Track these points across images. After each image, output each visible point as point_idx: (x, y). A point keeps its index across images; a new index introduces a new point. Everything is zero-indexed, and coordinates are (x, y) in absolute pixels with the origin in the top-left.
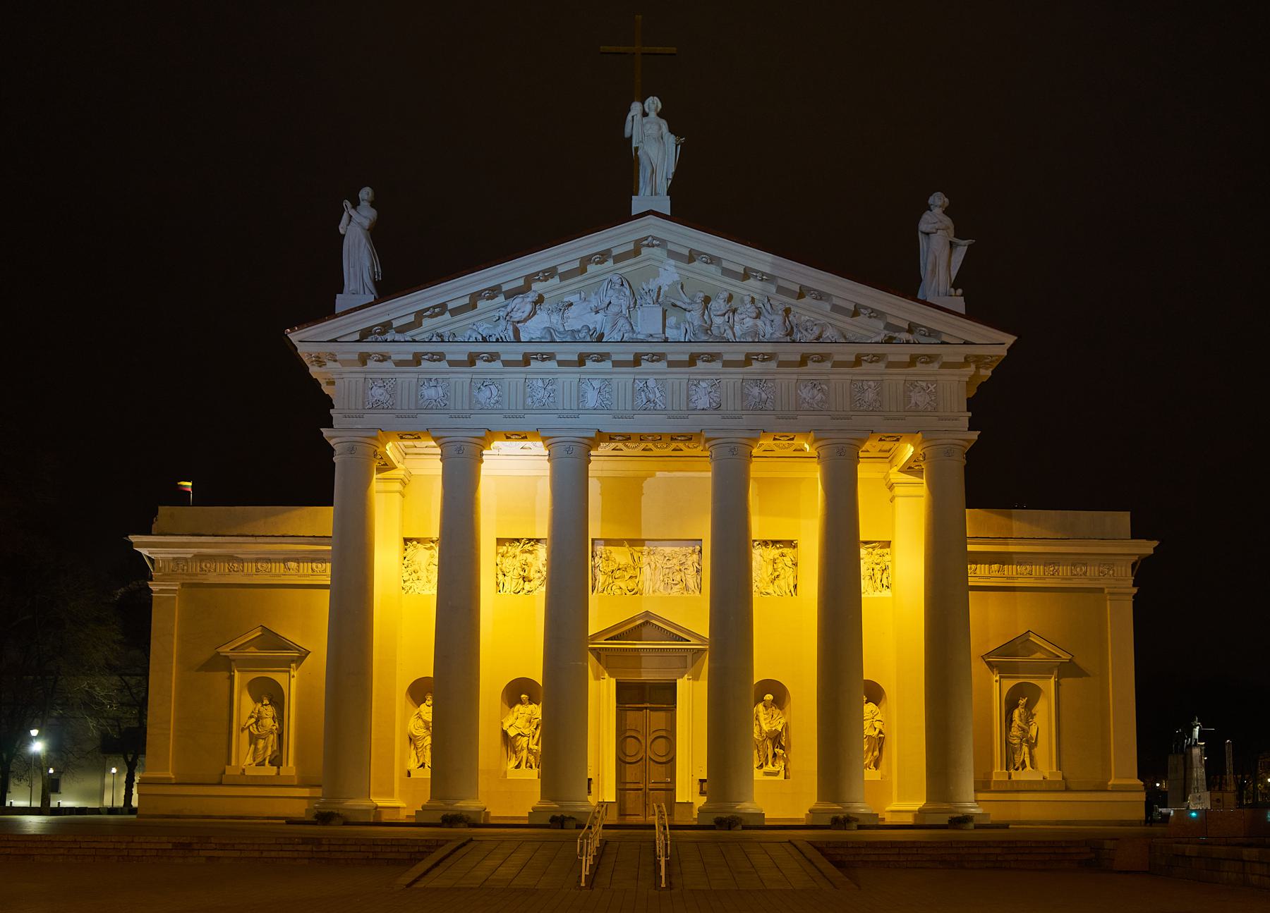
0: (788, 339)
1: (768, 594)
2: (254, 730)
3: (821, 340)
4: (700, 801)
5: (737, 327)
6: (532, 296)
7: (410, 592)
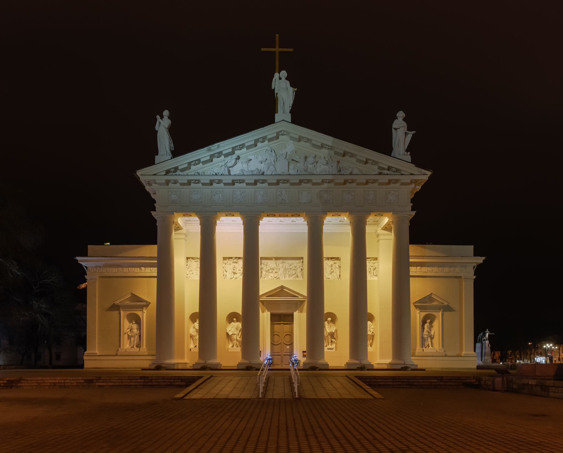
0: (339, 173)
1: (329, 279)
2: (129, 333)
4: (303, 360)
5: (318, 169)
7: (189, 279)
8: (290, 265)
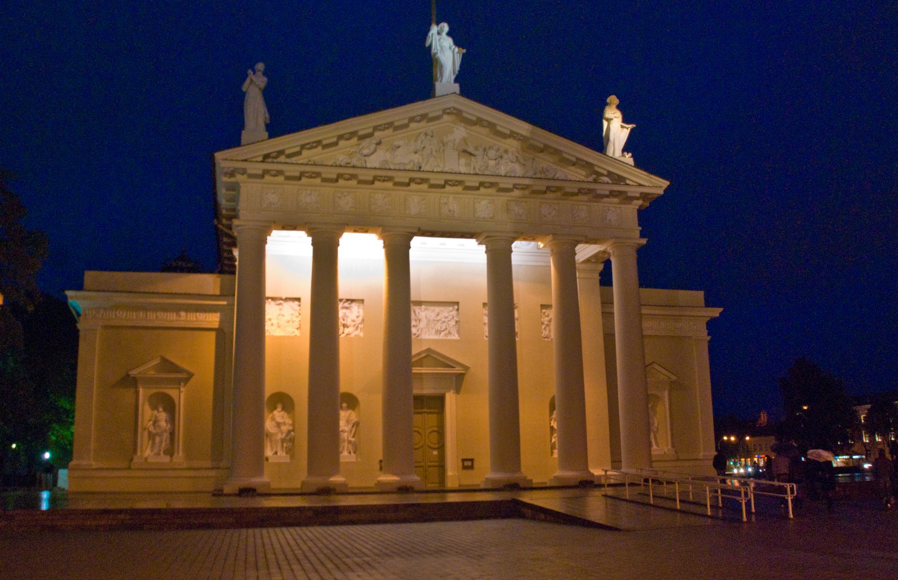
3: (555, 178)
6: (374, 140)
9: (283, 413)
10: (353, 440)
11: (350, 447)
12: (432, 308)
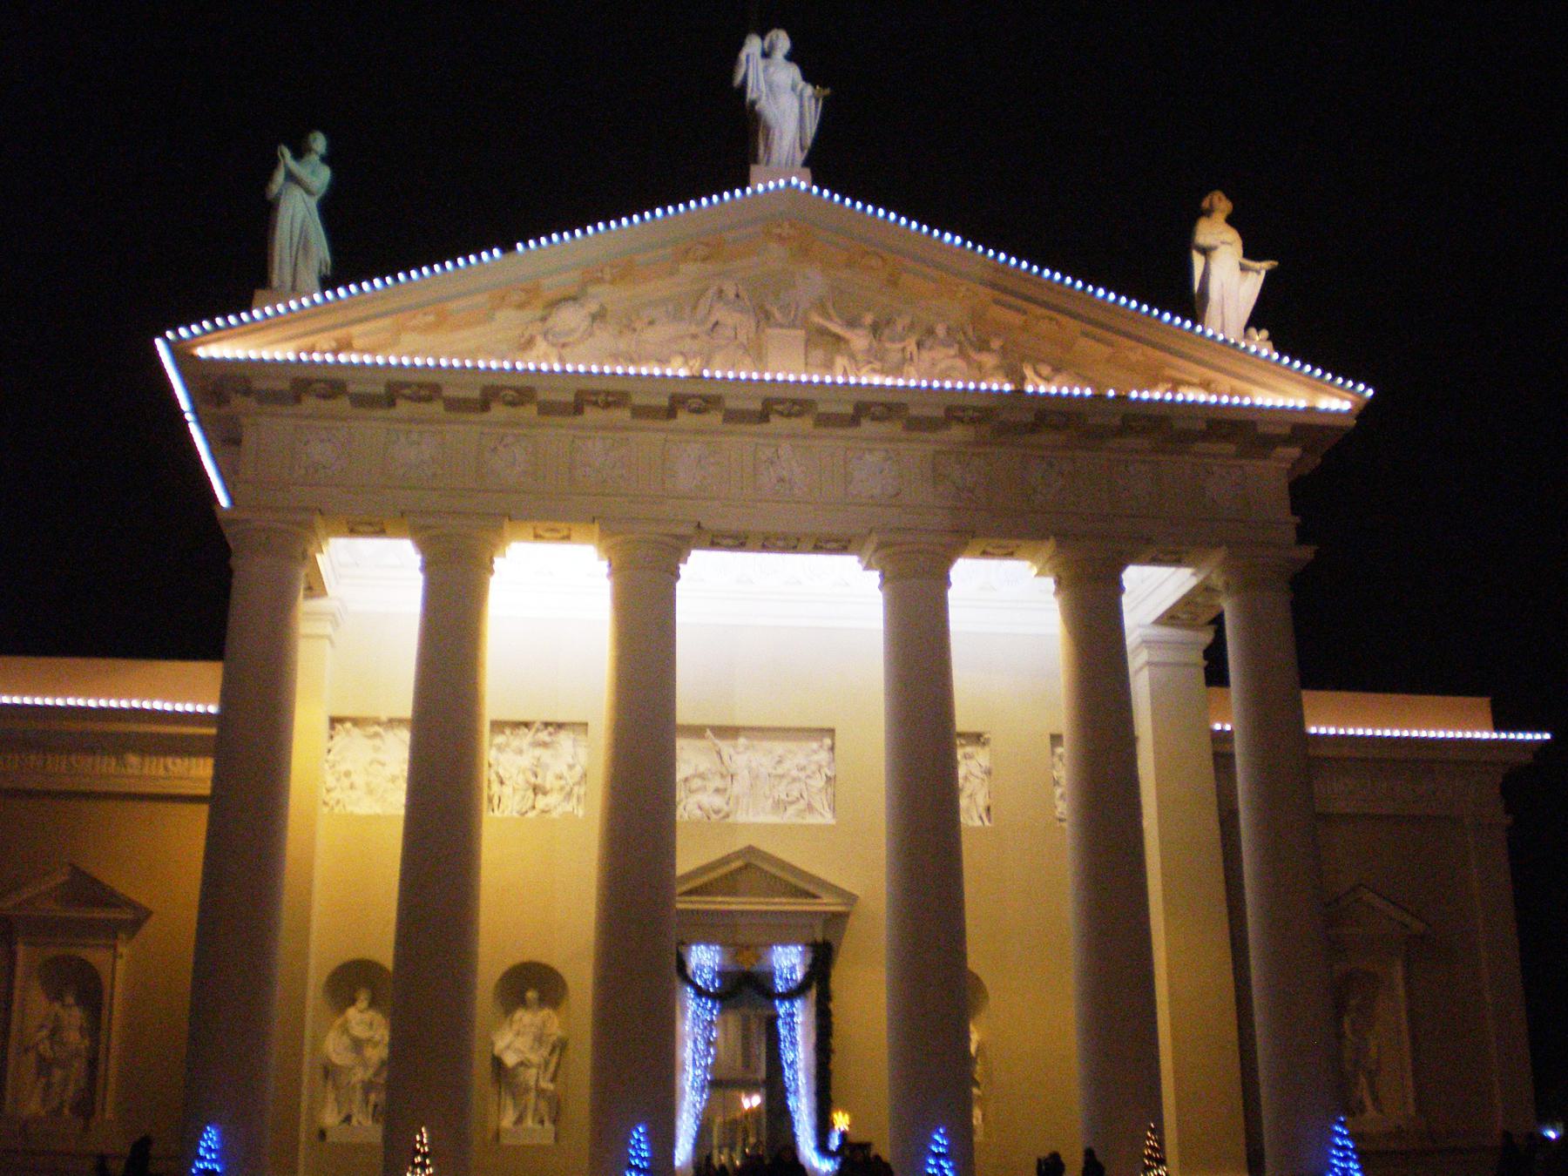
2: (45, 1048)
8: (780, 762)
9: (371, 1014)
10: (551, 1087)
11: (543, 1105)
12: (767, 744)
